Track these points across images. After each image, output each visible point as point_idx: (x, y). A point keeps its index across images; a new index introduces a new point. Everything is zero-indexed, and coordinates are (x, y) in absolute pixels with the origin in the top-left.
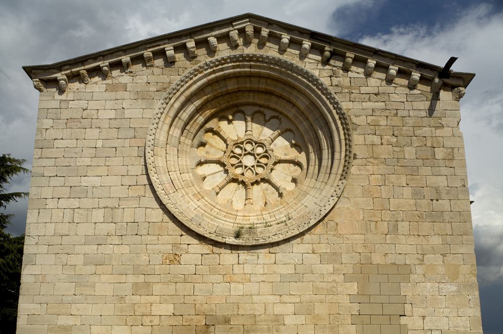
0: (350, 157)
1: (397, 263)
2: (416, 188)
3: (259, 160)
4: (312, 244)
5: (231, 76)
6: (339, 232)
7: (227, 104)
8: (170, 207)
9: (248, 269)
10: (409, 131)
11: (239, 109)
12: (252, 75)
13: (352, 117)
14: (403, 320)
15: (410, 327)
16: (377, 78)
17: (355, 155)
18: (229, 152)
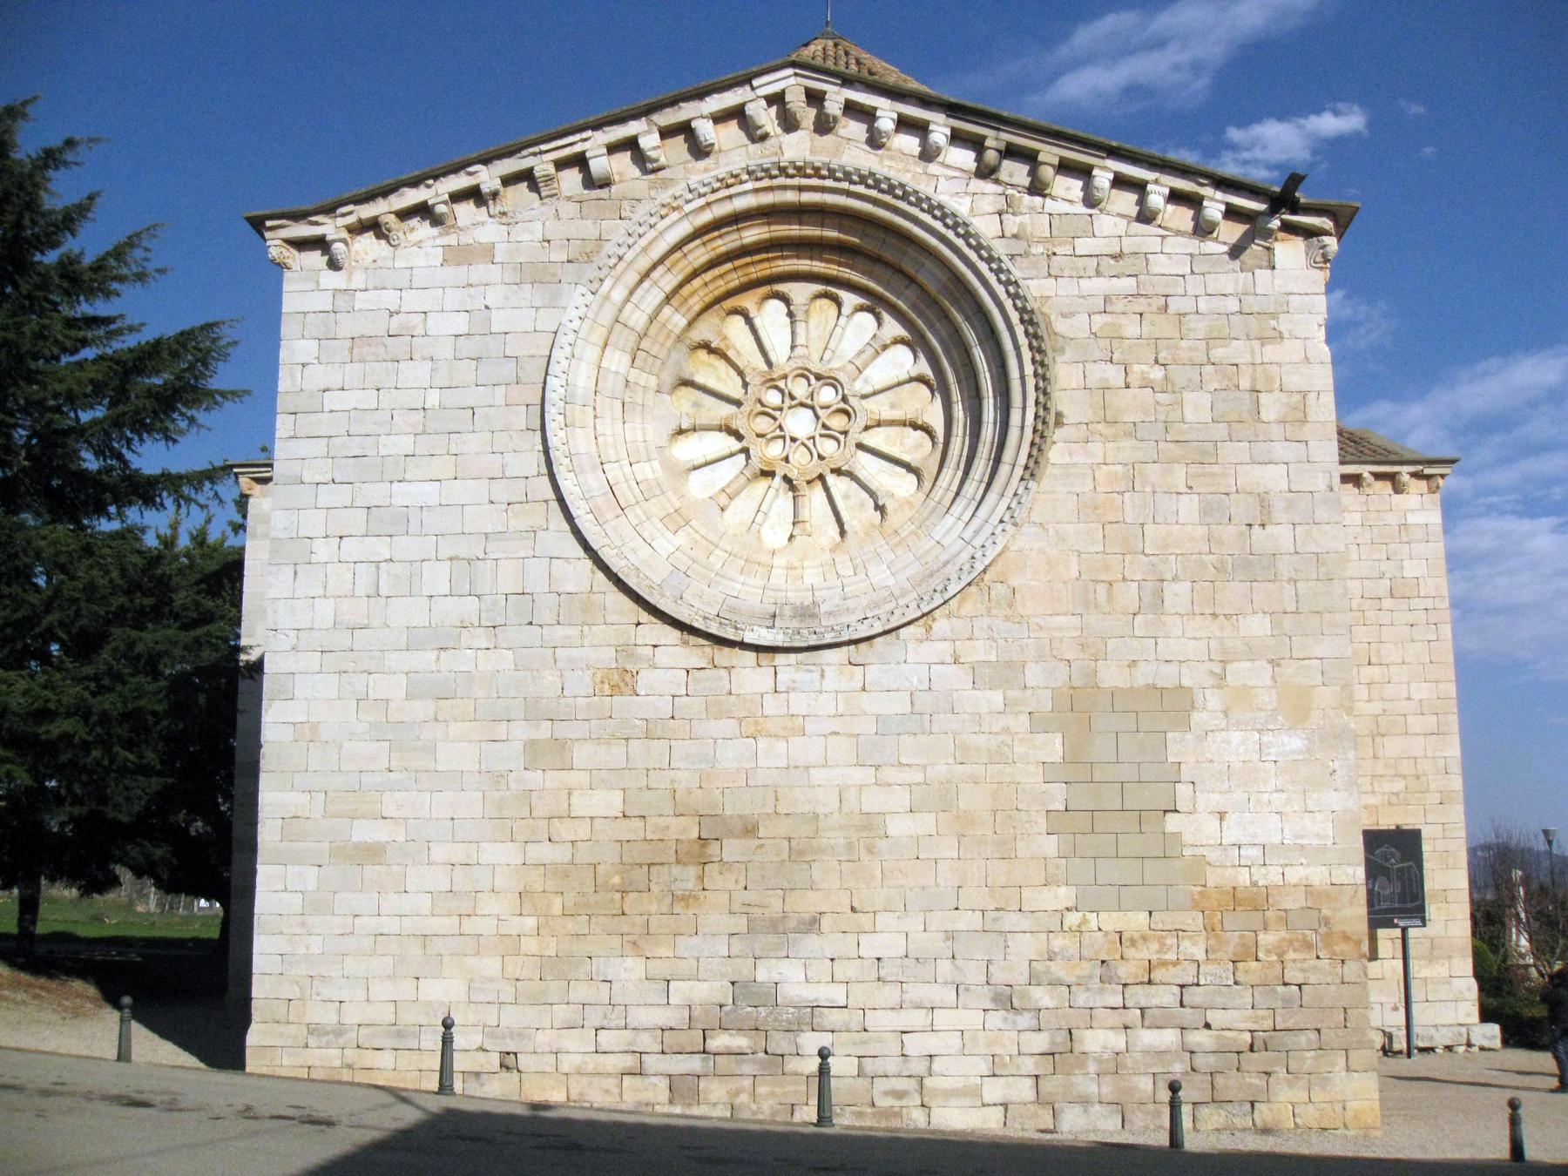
0: (1044, 423)
1: (1160, 684)
2: (1210, 497)
3: (828, 423)
4: (954, 641)
6: (1020, 609)
8: (607, 555)
9: (799, 703)
10: (1196, 349)
13: (1053, 318)
14: (1172, 823)
15: (1187, 838)
16: (1119, 215)
17: (1059, 415)
18: (751, 403)
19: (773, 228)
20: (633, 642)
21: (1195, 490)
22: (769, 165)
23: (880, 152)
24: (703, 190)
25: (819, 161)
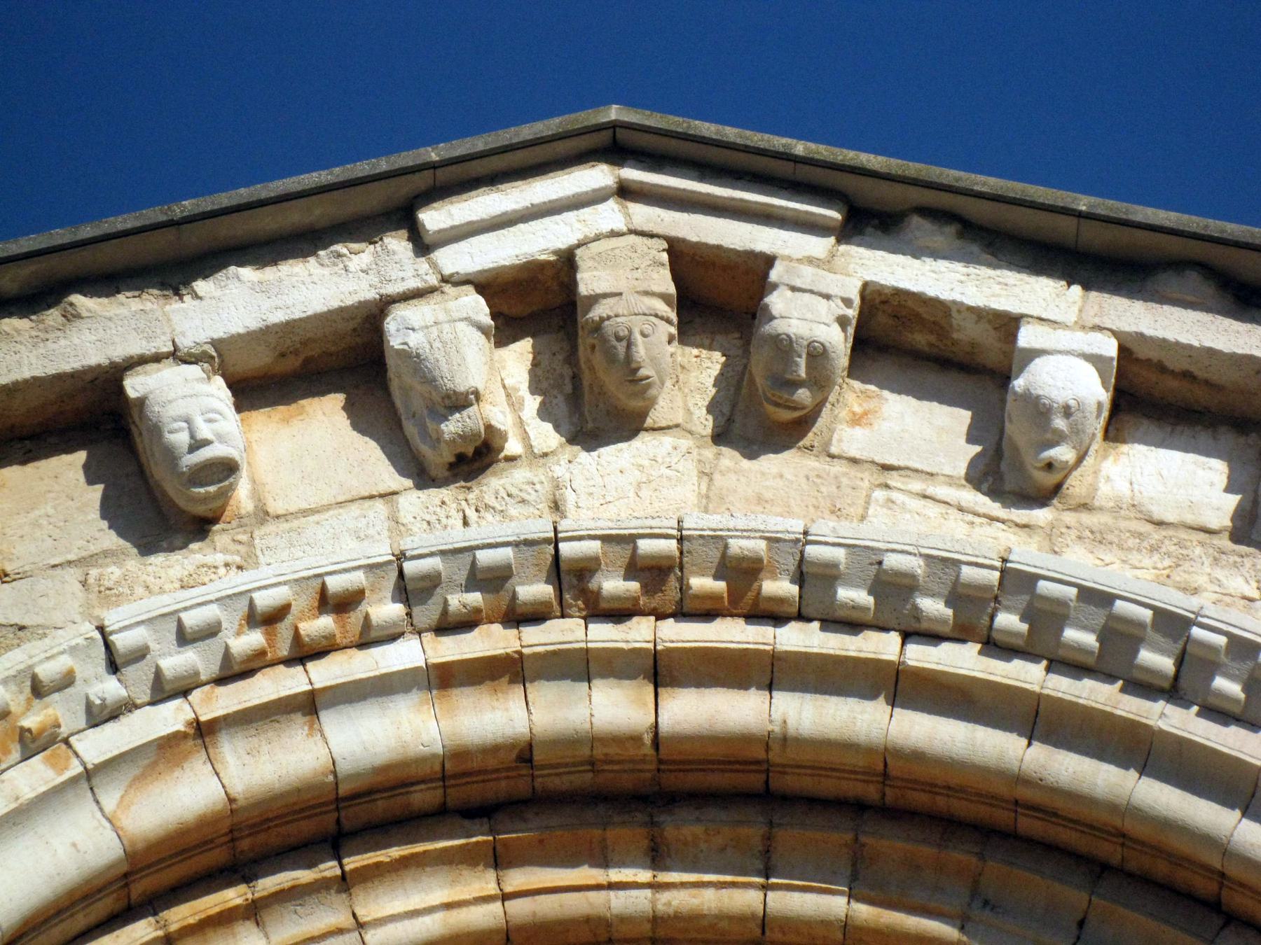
12: (673, 781)
19: (518, 879)
22: (505, 555)
23: (1041, 516)
24: (175, 662)
25: (747, 533)
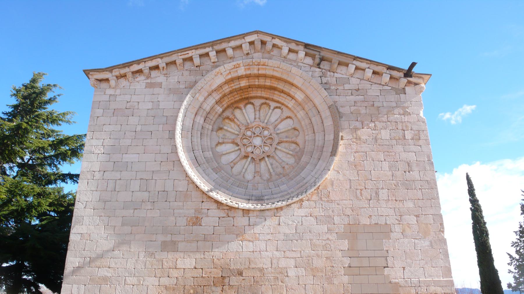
3: (266, 142)
5: (244, 76)
7: (240, 98)
11: (250, 101)
16: (357, 78)
20: (201, 208)
21: (386, 160)
